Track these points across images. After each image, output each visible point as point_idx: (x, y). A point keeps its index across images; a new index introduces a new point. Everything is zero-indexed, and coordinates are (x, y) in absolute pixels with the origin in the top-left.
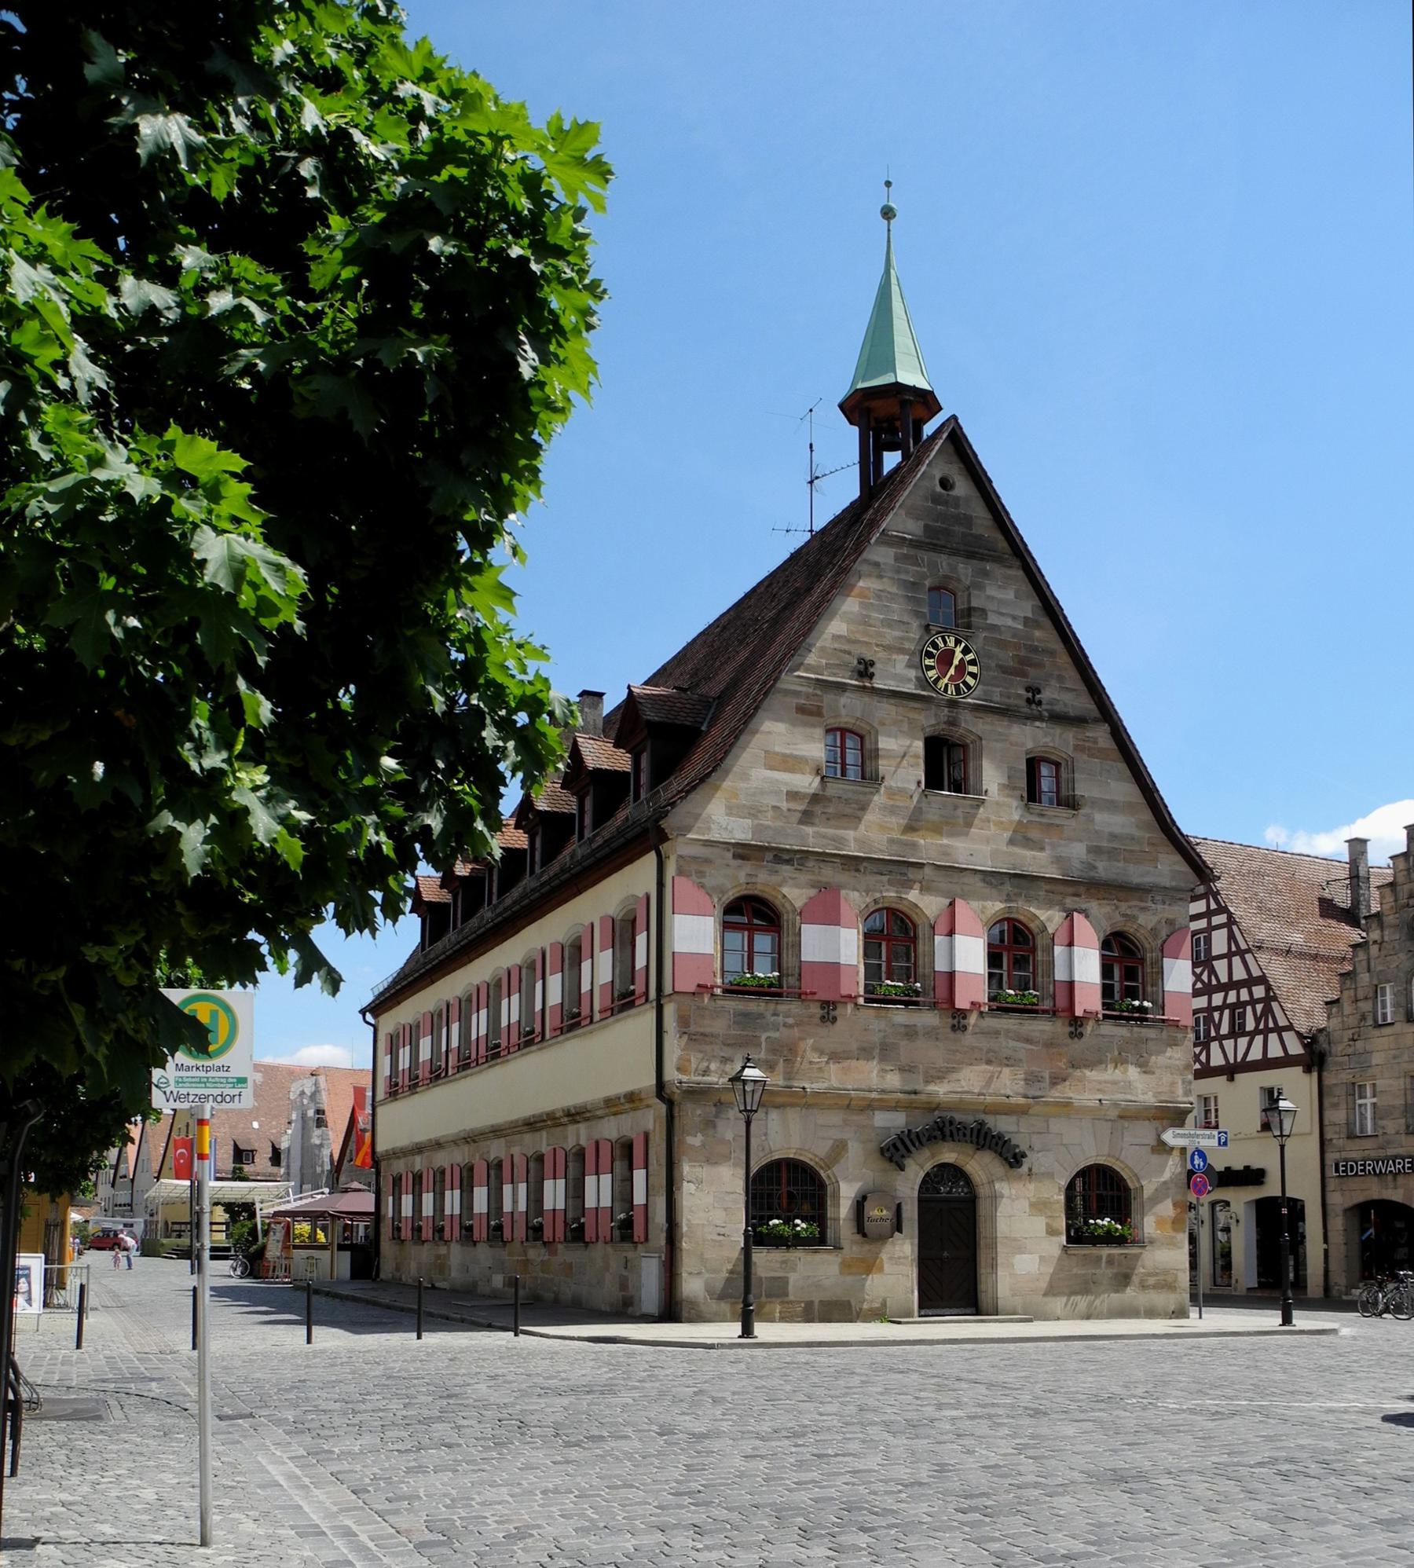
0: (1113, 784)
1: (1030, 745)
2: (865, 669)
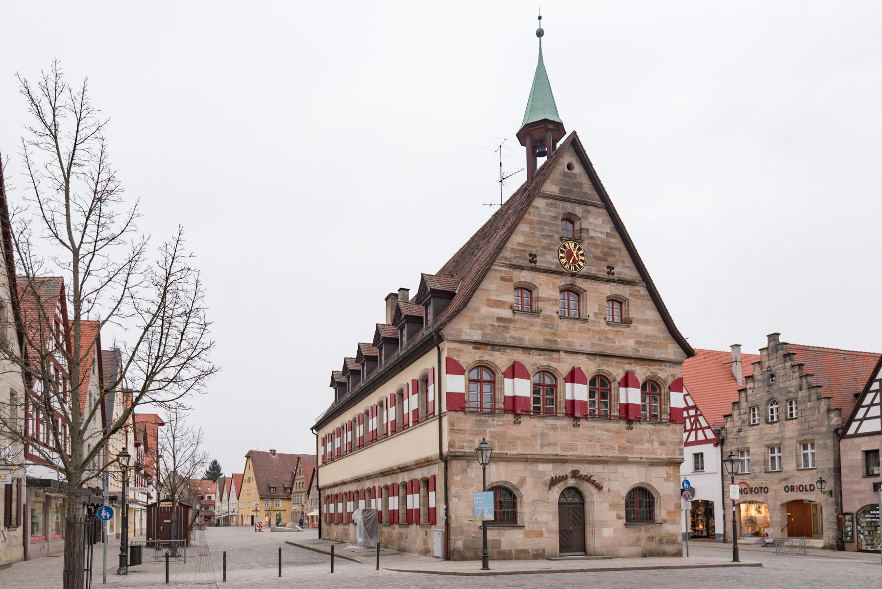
0: (647, 311)
1: (609, 294)
2: (533, 258)
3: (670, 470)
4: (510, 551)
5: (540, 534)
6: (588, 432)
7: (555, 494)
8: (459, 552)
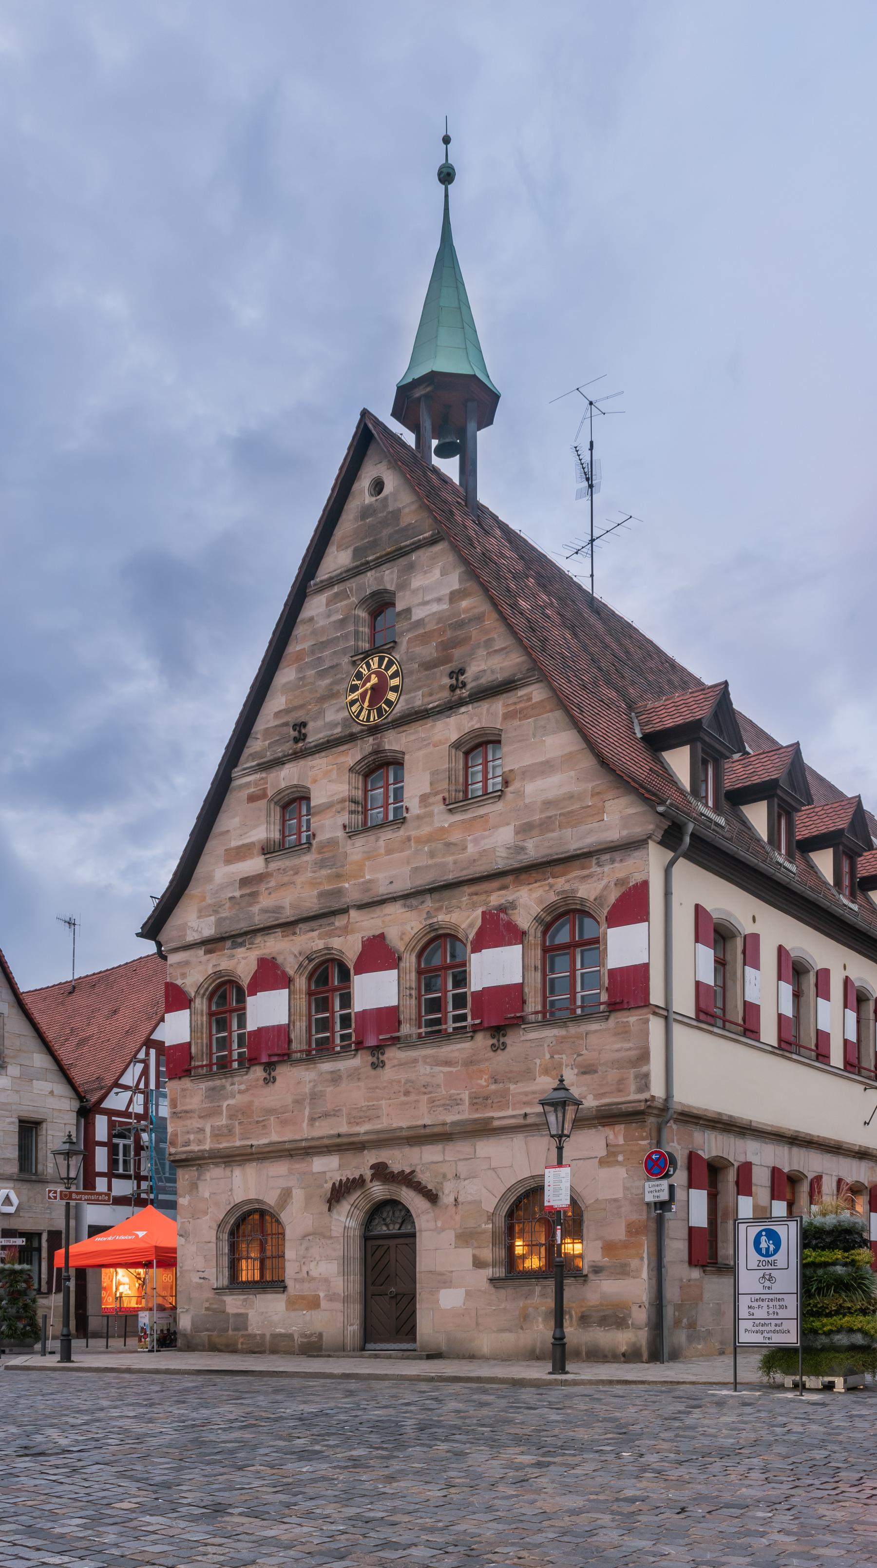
1: (454, 737)
3: (617, 1135)
4: (263, 1336)
5: (314, 1303)
6: (403, 1076)
7: (346, 1219)
8: (185, 1335)
